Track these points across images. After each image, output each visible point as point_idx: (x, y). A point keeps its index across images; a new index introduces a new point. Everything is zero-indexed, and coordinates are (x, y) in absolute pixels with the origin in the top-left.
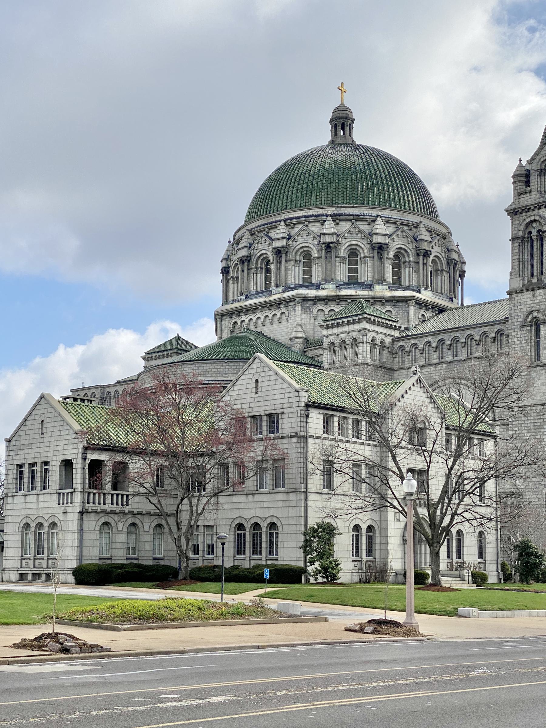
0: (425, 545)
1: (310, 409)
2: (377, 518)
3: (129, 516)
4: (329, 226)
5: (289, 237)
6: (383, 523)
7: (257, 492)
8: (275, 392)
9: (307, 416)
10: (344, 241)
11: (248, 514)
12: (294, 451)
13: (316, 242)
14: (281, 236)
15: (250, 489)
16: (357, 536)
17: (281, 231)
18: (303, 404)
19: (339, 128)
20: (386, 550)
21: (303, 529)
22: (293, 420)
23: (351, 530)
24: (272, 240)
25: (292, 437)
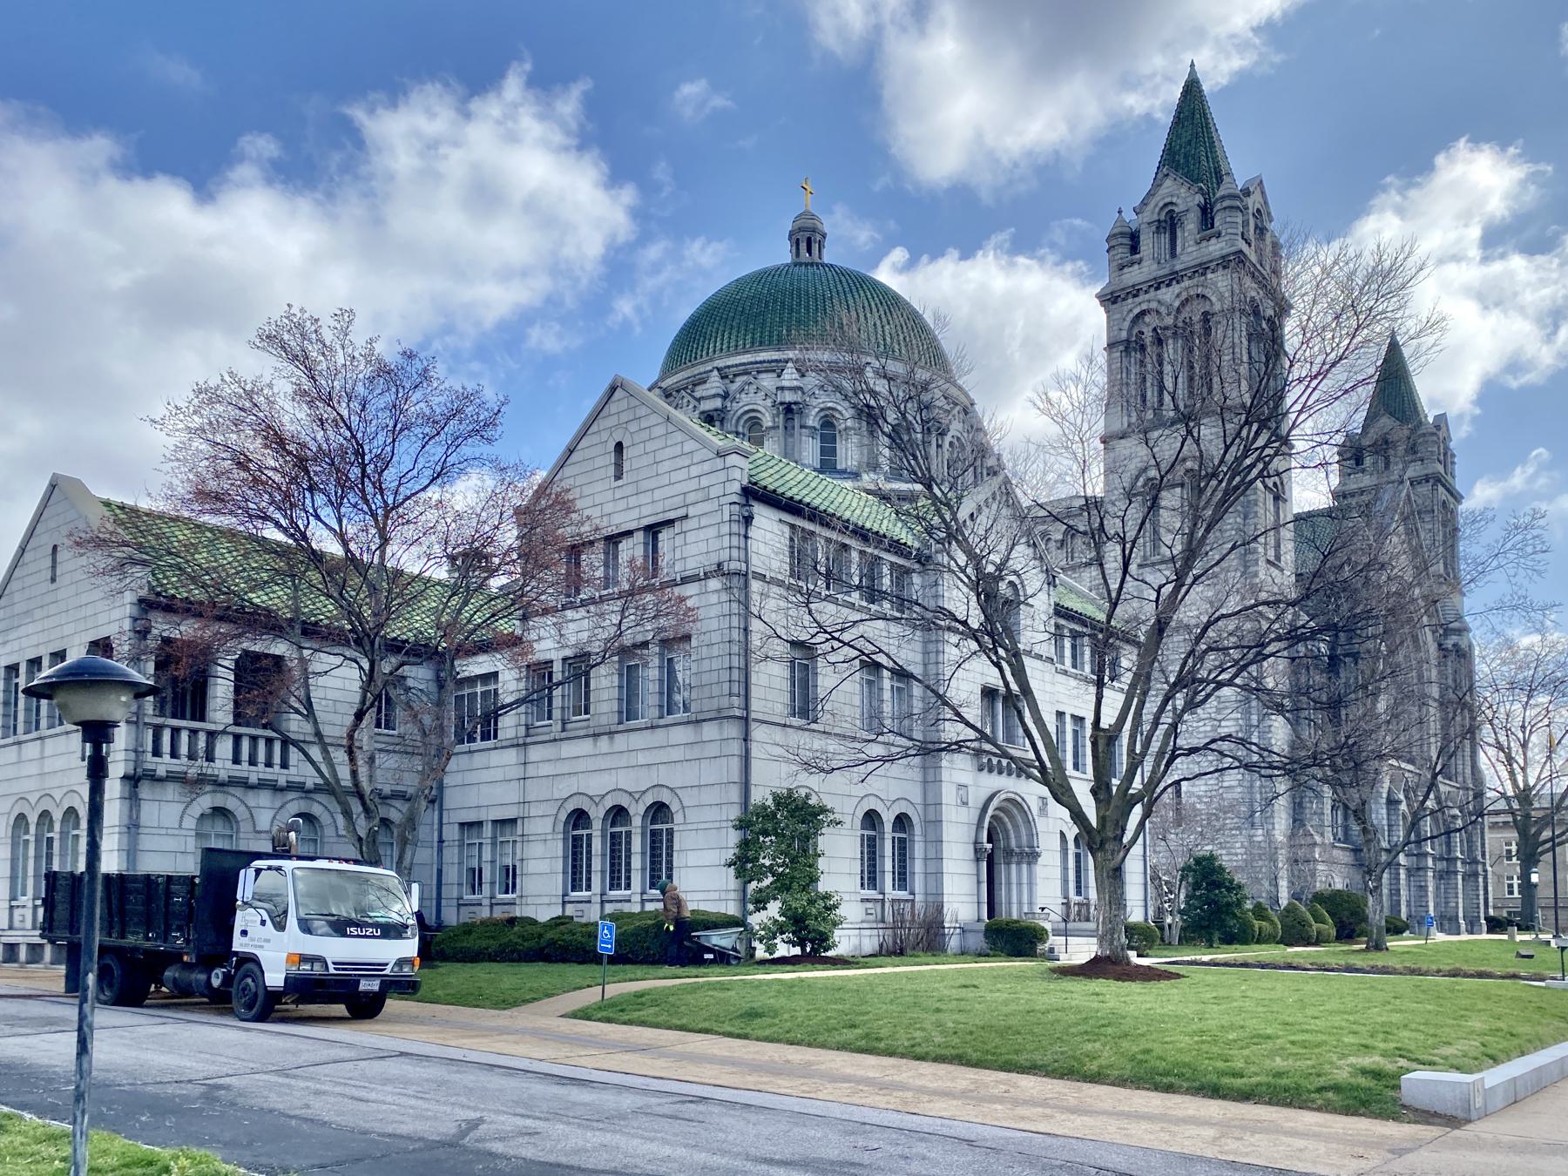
0: (1019, 863)
1: (752, 502)
2: (917, 798)
3: (291, 795)
4: (790, 377)
5: (725, 396)
6: (931, 808)
7: (621, 727)
8: (666, 466)
9: (748, 520)
10: (814, 402)
11: (597, 785)
12: (714, 611)
13: (769, 402)
14: (713, 392)
15: (604, 720)
16: (872, 840)
17: (714, 384)
18: (736, 487)
19: (803, 246)
20: (939, 873)
21: (735, 813)
22: (712, 532)
23: (858, 823)
24: (699, 400)
25: (707, 576)
